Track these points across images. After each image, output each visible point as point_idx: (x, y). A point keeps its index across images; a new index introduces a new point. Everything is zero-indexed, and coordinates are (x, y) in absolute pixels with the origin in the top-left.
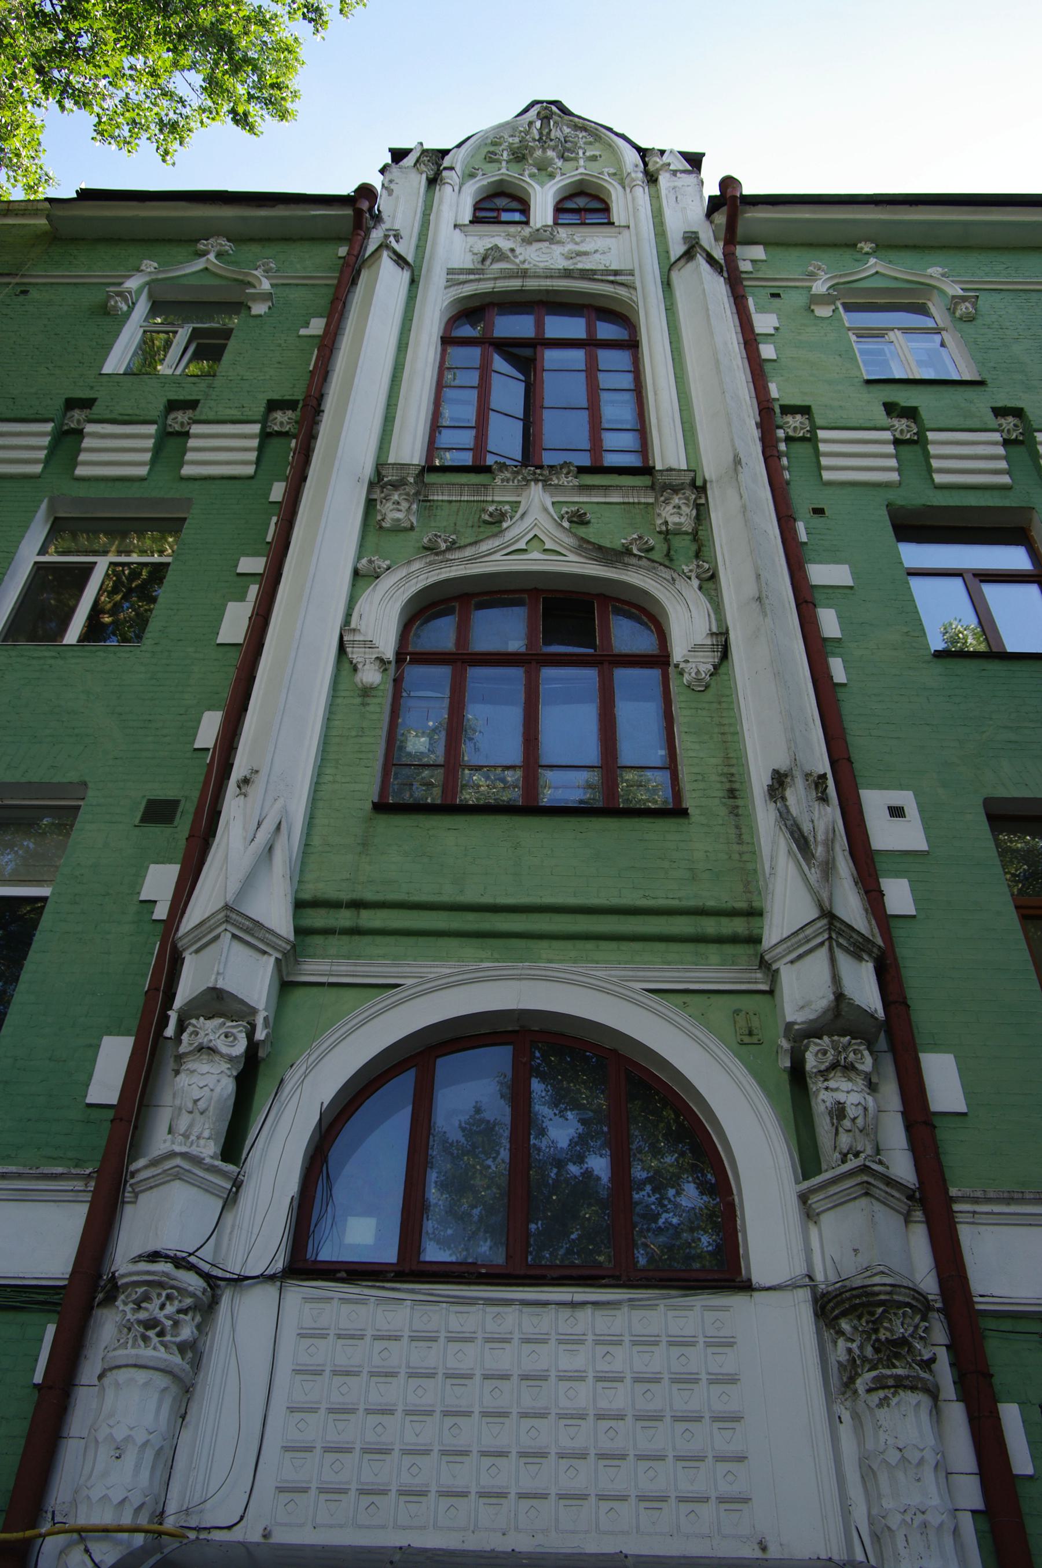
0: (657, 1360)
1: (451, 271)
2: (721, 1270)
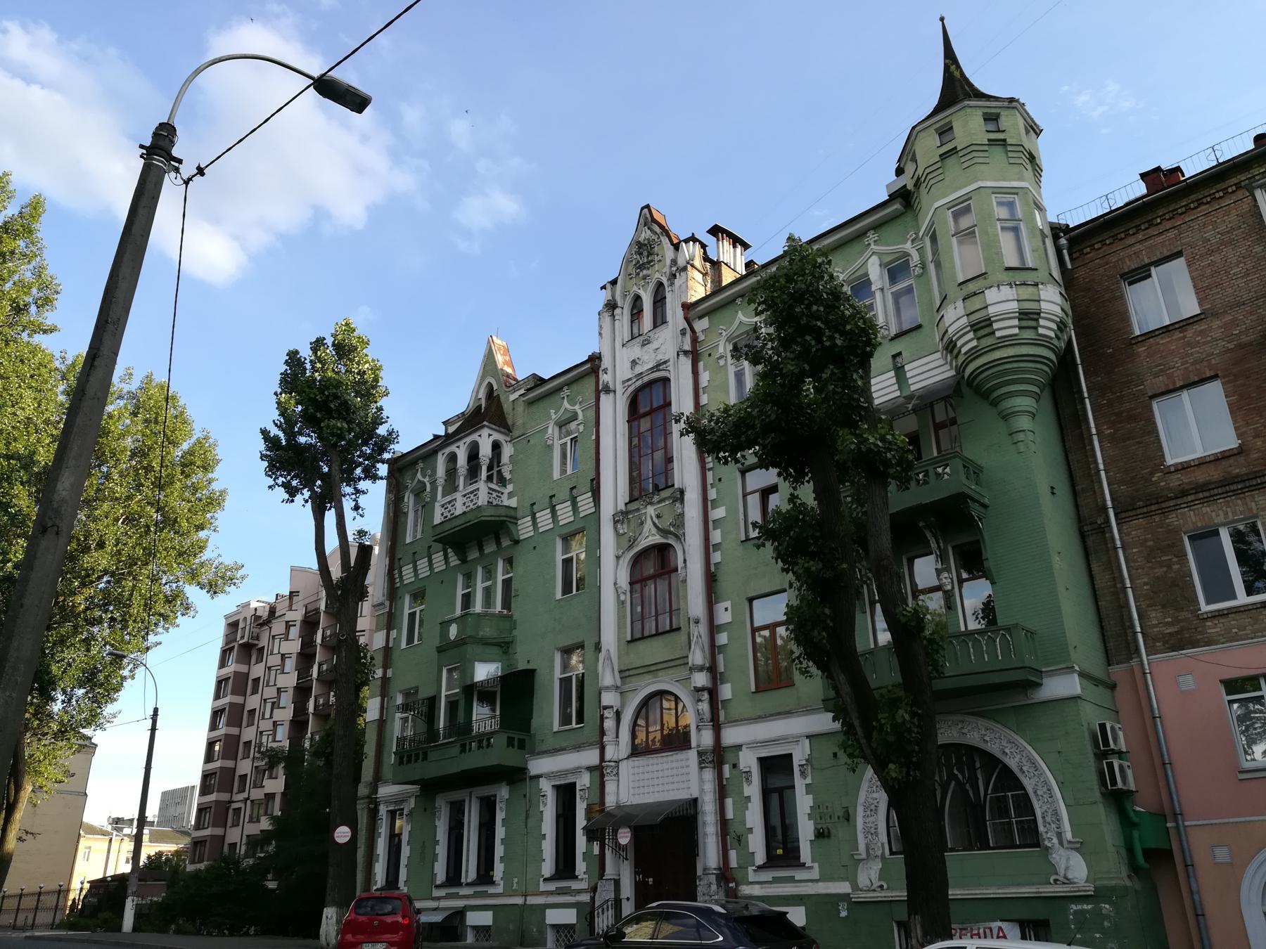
0: (680, 764)
1: (624, 382)
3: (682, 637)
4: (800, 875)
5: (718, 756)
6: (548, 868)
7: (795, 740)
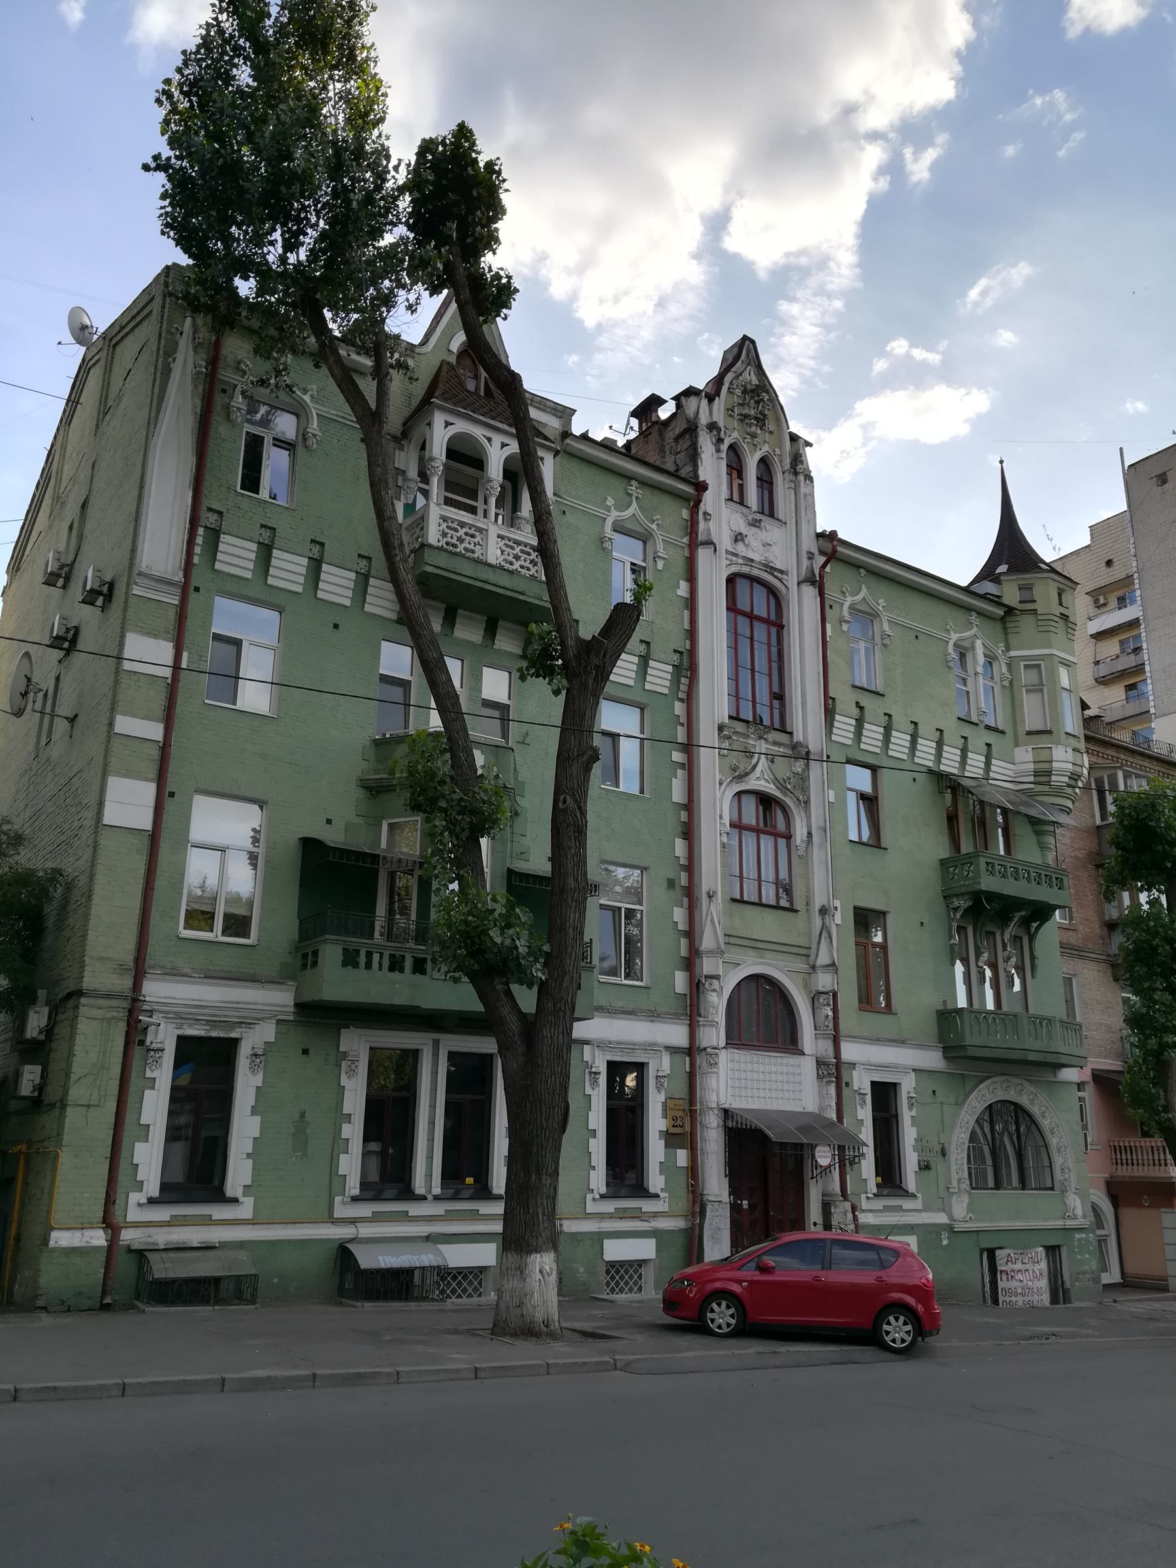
1: (727, 552)
2: (790, 1043)
3: (799, 921)
4: (907, 1204)
5: (834, 1071)
6: (598, 1179)
7: (904, 1070)
